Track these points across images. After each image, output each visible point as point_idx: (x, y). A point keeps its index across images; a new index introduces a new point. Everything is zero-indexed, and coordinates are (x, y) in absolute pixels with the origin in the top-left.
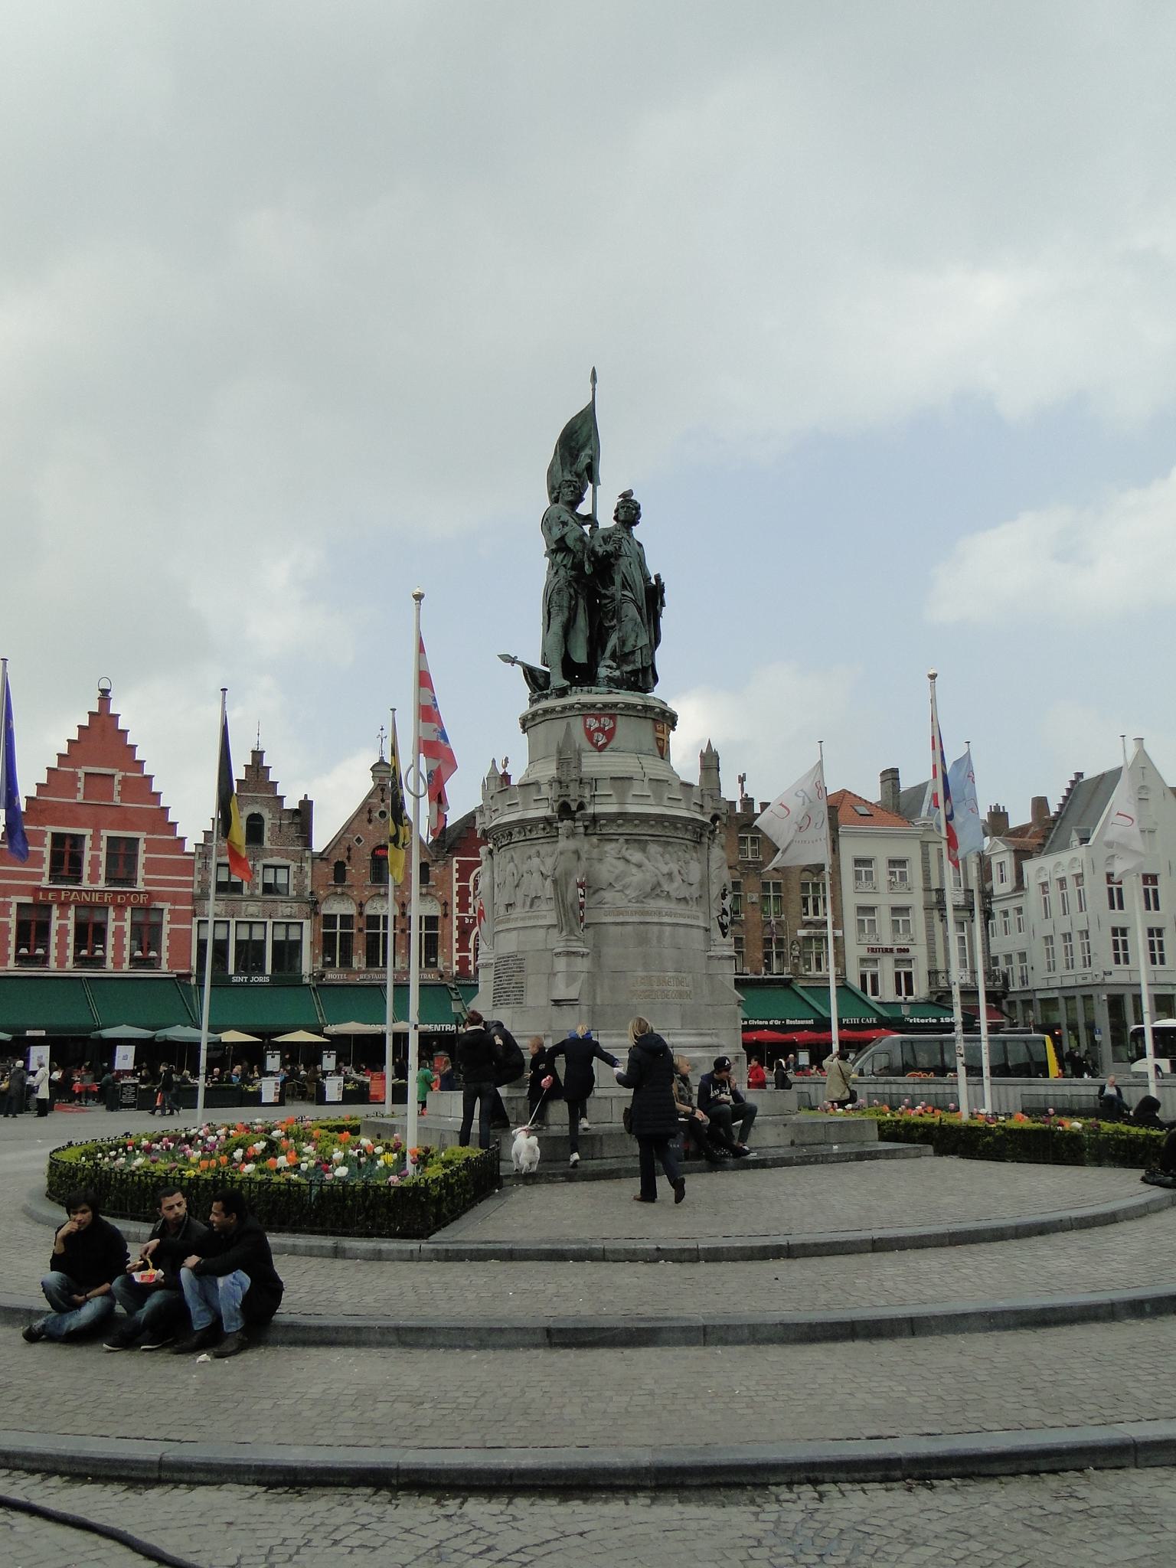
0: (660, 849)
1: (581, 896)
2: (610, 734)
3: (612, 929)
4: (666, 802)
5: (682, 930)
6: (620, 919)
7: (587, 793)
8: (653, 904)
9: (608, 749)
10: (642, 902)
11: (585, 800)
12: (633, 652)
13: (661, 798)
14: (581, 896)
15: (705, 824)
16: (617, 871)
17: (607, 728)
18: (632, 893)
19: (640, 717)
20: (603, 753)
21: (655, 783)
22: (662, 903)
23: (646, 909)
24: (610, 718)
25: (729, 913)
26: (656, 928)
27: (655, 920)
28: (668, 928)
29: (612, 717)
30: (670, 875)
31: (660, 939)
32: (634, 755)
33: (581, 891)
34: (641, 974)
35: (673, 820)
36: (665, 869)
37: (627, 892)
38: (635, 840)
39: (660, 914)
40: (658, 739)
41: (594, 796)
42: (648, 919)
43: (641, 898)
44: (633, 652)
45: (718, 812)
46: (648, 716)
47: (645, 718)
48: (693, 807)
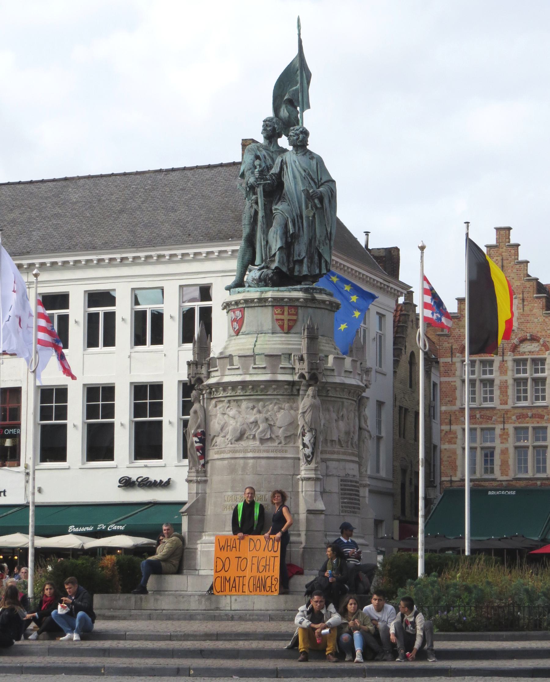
0: (251, 405)
1: (196, 442)
2: (240, 322)
3: (218, 463)
4: (251, 371)
5: (263, 462)
6: (222, 456)
7: (204, 371)
8: (243, 443)
9: (240, 334)
10: (235, 444)
11: (202, 376)
12: (275, 255)
13: (248, 369)
14: (196, 442)
15: (292, 384)
16: (222, 423)
17: (238, 318)
18: (229, 437)
19: (262, 306)
20: (238, 337)
21: (243, 358)
22: (251, 443)
23: (236, 449)
24: (240, 311)
25: (309, 445)
26: (242, 461)
27: (241, 455)
28: (251, 461)
29: (242, 310)
30: (256, 423)
31: (244, 468)
32: (256, 335)
33: (196, 439)
34: (230, 493)
35: (255, 385)
36: (252, 419)
37: (227, 437)
38: (234, 400)
39: (246, 451)
40: (277, 320)
41: (211, 372)
42: (237, 455)
43: (233, 441)
44: (275, 255)
45: (303, 372)
46: (267, 304)
47: (265, 306)
48: (280, 371)
